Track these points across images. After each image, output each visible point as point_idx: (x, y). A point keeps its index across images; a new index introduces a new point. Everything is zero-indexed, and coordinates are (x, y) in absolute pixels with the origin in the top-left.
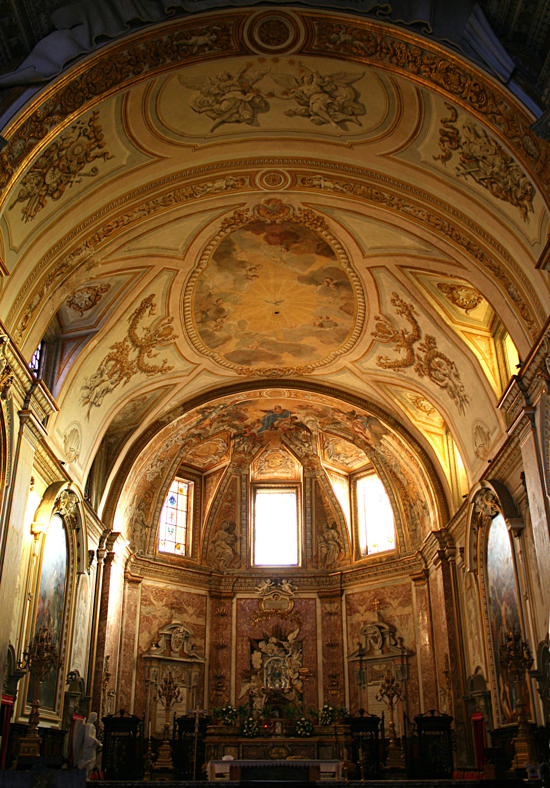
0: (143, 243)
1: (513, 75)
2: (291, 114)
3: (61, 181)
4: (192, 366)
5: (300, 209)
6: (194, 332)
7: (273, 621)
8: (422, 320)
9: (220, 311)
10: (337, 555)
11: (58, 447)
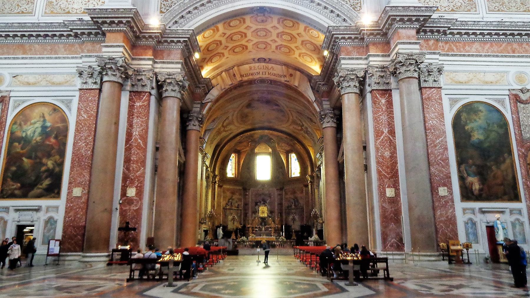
7: (262, 196)
8: (304, 123)
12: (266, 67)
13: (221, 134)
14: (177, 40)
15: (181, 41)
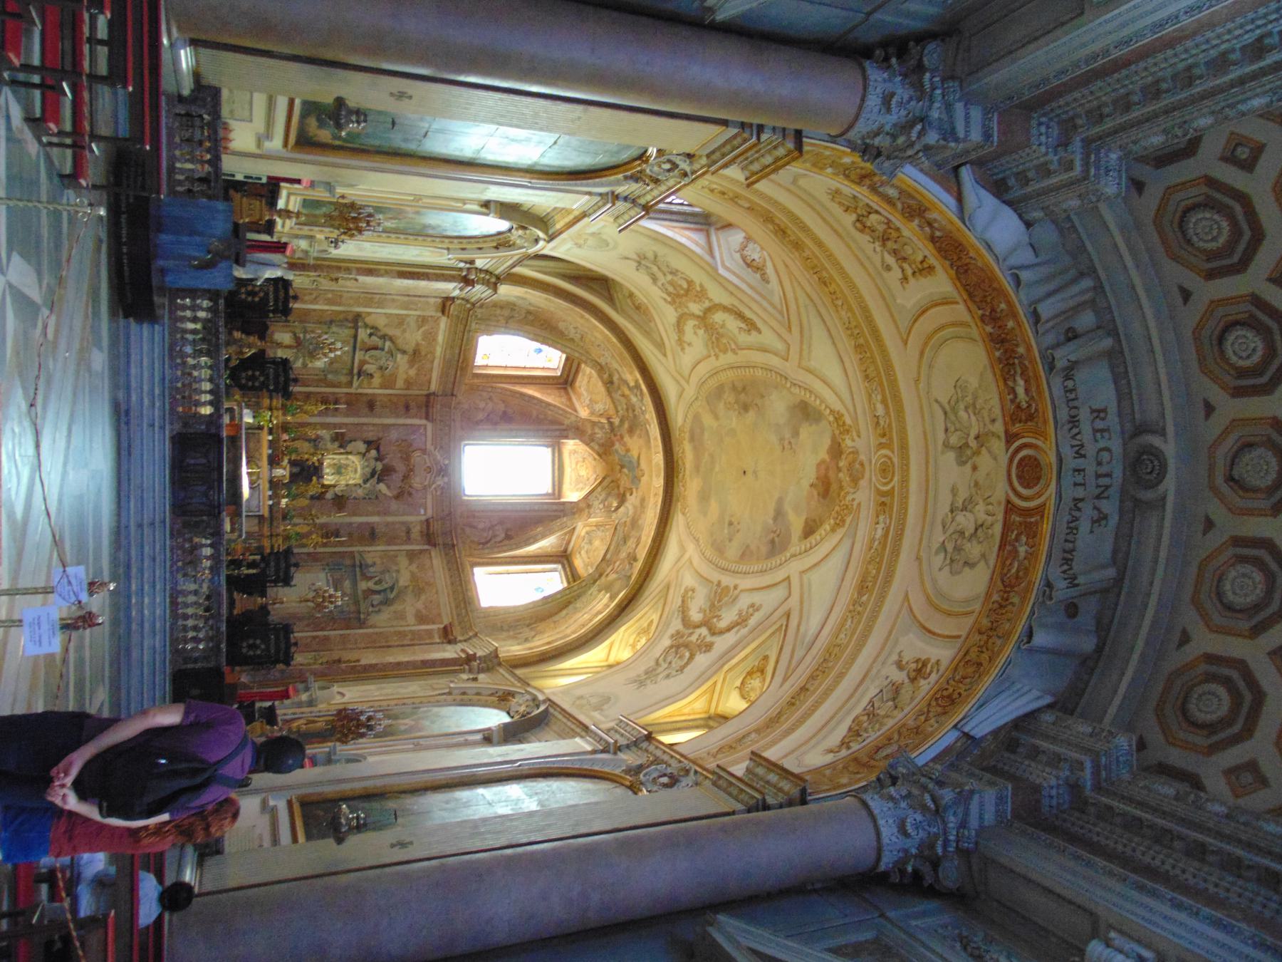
0: (815, 321)
1: (966, 735)
2: (954, 491)
3: (873, 231)
4: (686, 373)
5: (853, 500)
6: (723, 377)
7: (401, 467)
8: (731, 638)
9: (745, 408)
11: (587, 226)
12: (1107, 487)
13: (672, 303)
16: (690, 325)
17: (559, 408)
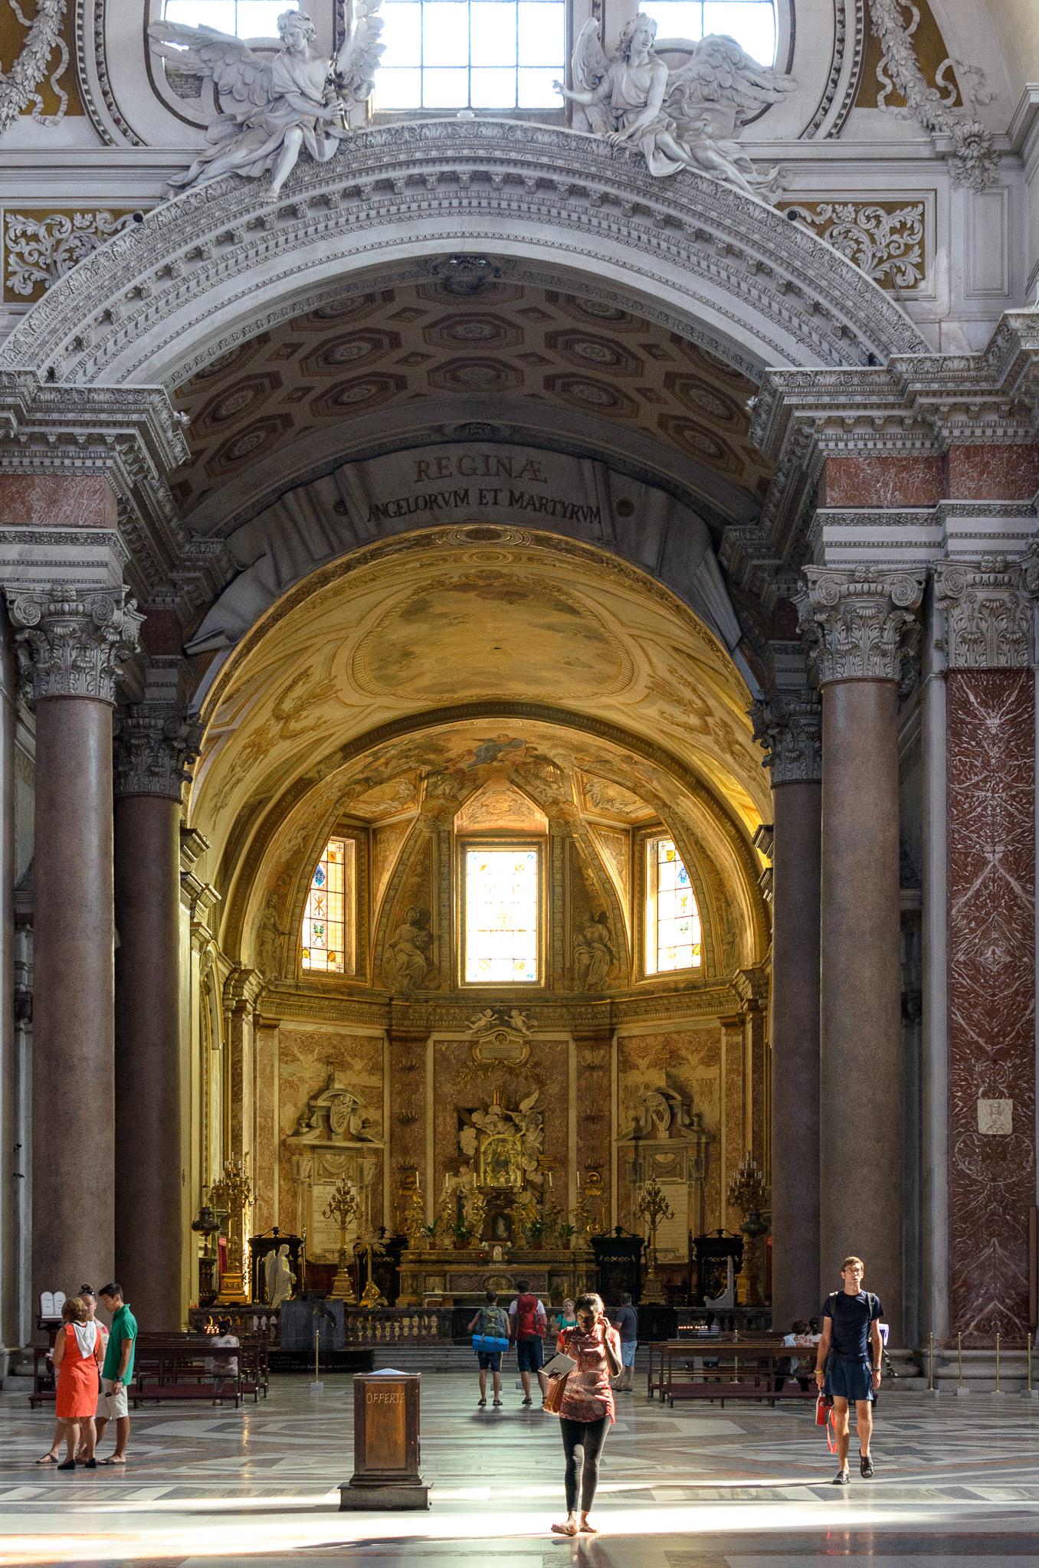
8: (711, 702)
10: (606, 968)
13: (266, 752)
14: (90, 436)
15: (109, 440)
16: (294, 726)
17: (405, 846)
